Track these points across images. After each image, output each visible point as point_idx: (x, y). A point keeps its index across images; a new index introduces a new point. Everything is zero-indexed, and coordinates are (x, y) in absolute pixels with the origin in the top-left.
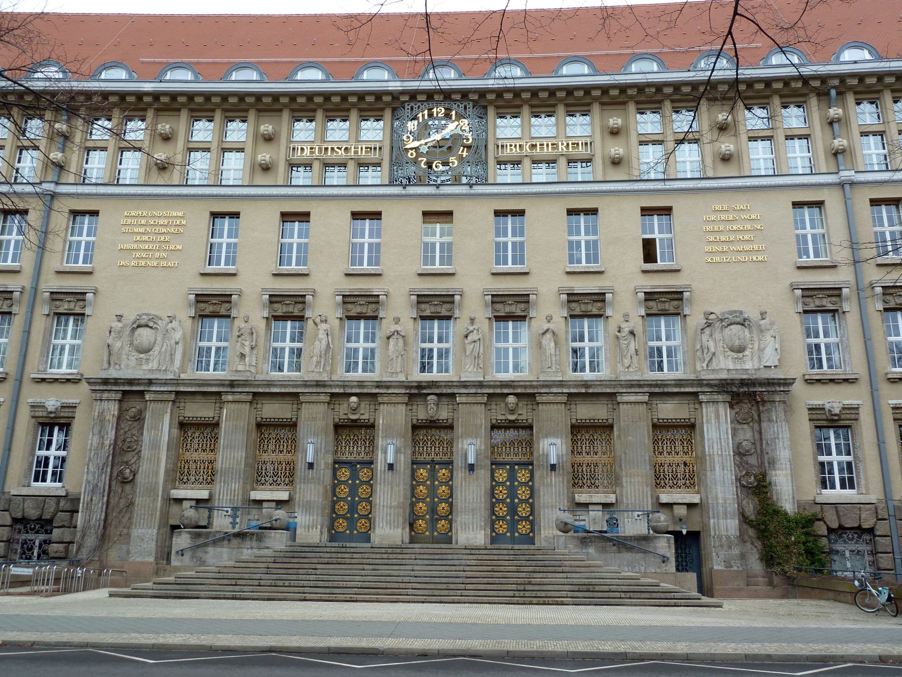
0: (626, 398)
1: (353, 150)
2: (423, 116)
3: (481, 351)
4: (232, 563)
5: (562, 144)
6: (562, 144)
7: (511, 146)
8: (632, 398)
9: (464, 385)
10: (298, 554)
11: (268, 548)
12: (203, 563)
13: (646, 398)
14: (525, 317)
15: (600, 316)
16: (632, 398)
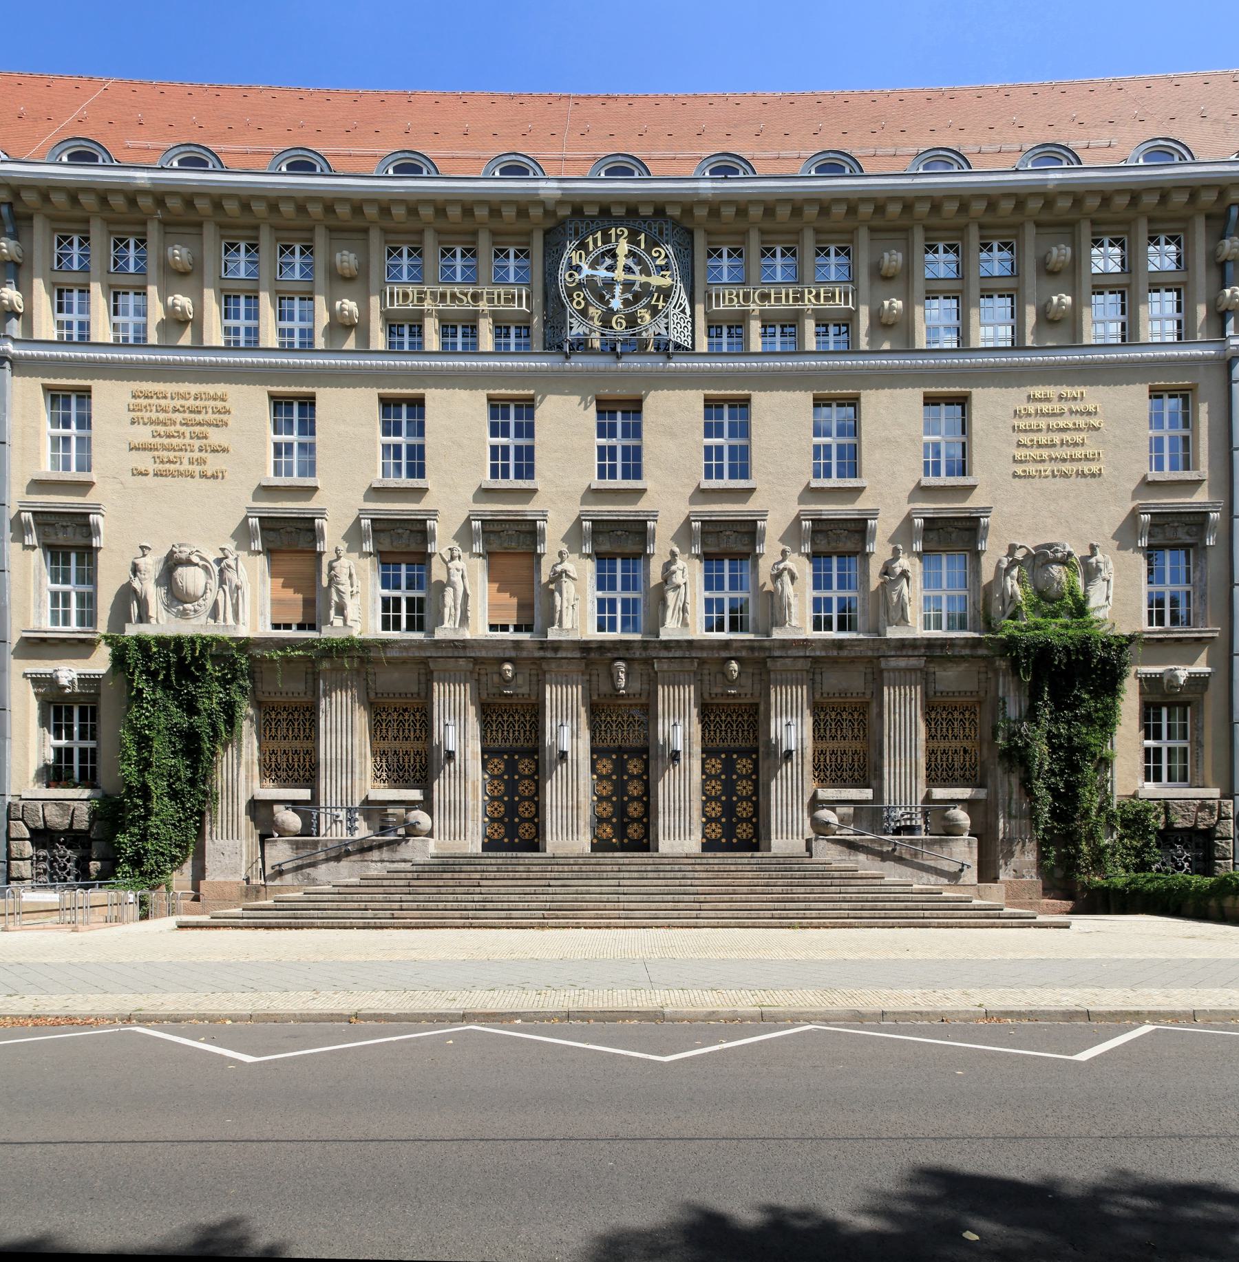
0: (893, 663)
1: (485, 296)
2: (595, 241)
3: (688, 600)
4: (355, 880)
5: (810, 292)
6: (810, 292)
7: (730, 294)
8: (902, 663)
9: (667, 645)
10: (447, 865)
11: (405, 861)
12: (314, 882)
13: (921, 662)
14: (748, 555)
15: (855, 554)
16: (902, 663)
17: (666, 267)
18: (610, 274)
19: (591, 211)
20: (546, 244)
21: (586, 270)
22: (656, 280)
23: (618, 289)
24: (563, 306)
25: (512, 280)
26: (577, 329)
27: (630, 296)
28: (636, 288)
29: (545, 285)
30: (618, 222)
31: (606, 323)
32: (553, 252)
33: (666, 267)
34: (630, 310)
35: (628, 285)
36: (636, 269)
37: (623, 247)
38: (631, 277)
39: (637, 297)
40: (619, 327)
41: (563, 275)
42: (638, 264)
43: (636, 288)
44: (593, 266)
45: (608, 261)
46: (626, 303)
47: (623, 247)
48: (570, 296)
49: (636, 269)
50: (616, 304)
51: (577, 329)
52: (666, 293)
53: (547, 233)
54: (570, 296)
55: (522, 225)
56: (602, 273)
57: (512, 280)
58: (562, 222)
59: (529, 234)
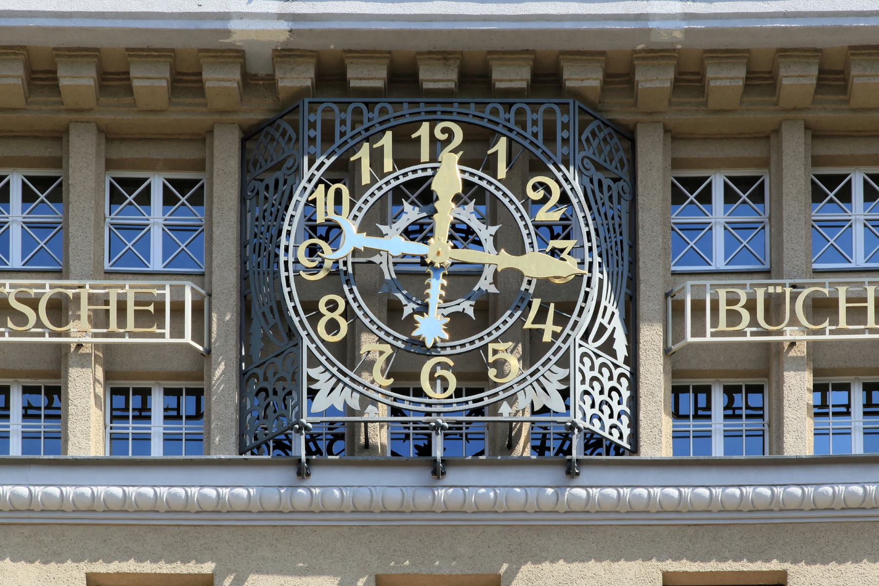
2: (376, 158)
17: (564, 229)
18: (416, 248)
19: (368, 76)
20: (246, 164)
21: (353, 238)
22: (536, 265)
23: (436, 287)
24: (292, 333)
25: (156, 263)
26: (328, 397)
27: (467, 307)
28: (485, 284)
29: (244, 278)
30: (438, 105)
31: (404, 381)
32: (265, 187)
33: (564, 229)
34: (469, 344)
35: (462, 278)
36: (486, 233)
37: (449, 177)
38: (469, 255)
39: (487, 312)
40: (438, 389)
41: (293, 248)
42: (490, 219)
43: (485, 284)
44: (369, 226)
45: (411, 213)
46: (458, 325)
47: (449, 177)
48: (310, 307)
49: (486, 233)
50: (431, 327)
51: (328, 397)
52: (563, 300)
53: (250, 135)
54: (310, 307)
55: (185, 115)
56: (394, 244)
57: (156, 263)
58: (290, 107)
59: (203, 138)
